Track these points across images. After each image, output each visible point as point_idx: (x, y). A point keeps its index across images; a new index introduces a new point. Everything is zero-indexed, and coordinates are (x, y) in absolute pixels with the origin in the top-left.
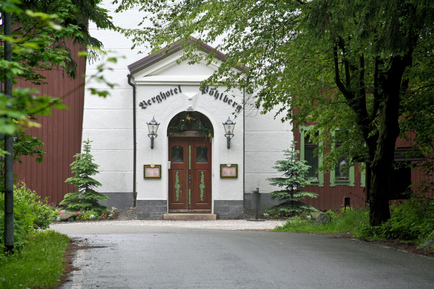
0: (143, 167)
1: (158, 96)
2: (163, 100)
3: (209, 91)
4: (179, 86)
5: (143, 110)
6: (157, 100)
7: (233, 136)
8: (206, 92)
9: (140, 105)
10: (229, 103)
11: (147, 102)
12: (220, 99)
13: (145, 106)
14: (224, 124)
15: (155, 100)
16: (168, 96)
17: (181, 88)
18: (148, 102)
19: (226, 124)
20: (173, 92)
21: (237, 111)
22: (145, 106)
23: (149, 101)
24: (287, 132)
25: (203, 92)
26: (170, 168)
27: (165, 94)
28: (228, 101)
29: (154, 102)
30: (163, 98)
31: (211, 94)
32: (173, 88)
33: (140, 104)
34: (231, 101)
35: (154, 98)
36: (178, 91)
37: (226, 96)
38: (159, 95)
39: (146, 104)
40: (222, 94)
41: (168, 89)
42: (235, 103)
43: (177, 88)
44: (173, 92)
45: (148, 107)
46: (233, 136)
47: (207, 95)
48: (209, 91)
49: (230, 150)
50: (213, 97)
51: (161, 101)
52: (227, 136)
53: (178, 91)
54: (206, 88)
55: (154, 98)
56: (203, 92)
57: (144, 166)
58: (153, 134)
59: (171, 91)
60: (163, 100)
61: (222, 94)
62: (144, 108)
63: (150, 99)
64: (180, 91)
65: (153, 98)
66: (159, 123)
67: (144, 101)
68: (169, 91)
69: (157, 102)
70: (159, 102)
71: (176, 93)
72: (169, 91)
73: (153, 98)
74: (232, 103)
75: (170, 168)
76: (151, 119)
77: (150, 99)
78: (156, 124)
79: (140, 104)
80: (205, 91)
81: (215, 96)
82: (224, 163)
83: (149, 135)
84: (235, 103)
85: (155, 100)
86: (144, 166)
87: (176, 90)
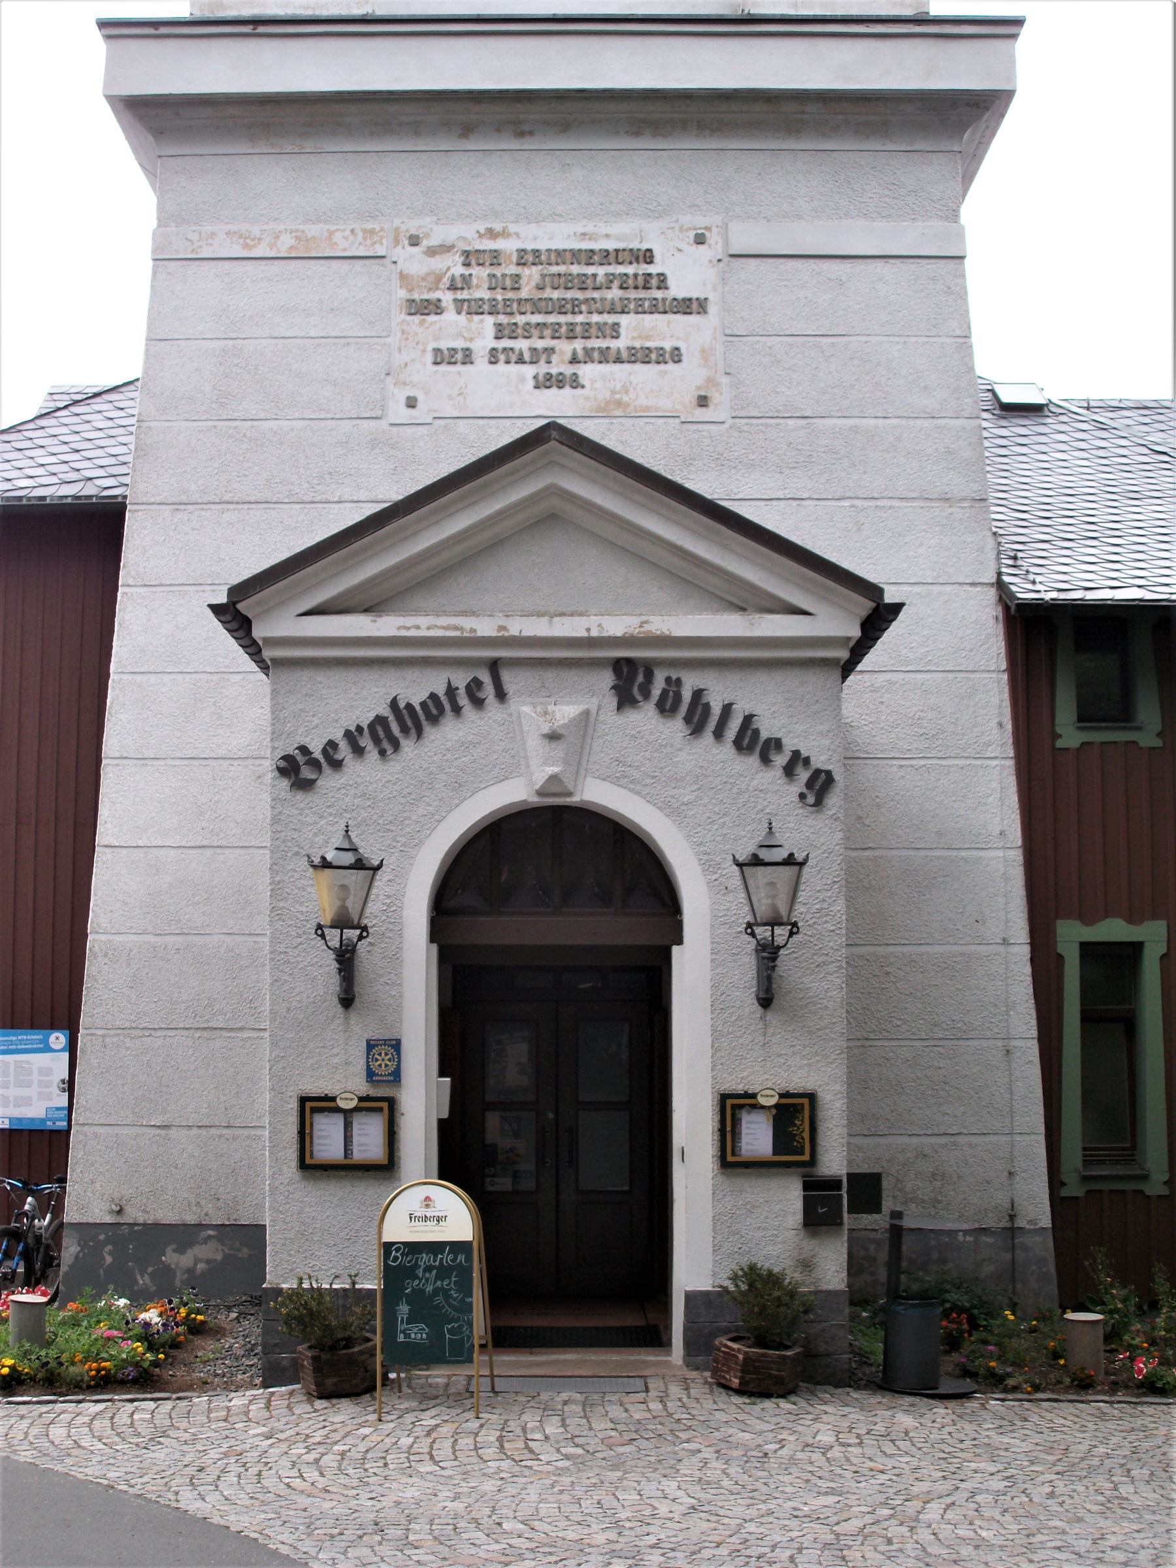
0: (294, 1105)
1: (380, 720)
2: (407, 745)
3: (656, 692)
4: (494, 666)
5: (300, 796)
6: (376, 741)
7: (791, 934)
8: (639, 698)
9: (282, 772)
10: (765, 760)
11: (317, 754)
12: (718, 734)
13: (307, 773)
14: (740, 865)
15: (366, 741)
16: (434, 720)
17: (506, 676)
18: (324, 751)
19: (756, 861)
20: (463, 700)
21: (811, 799)
22: (307, 773)
23: (332, 744)
24: (1001, 949)
25: (625, 699)
26: (445, 1115)
27: (418, 708)
28: (758, 749)
29: (358, 751)
30: (405, 730)
31: (667, 706)
32: (461, 680)
33: (283, 764)
34: (777, 744)
35: (359, 729)
36: (489, 691)
37: (748, 719)
38: (385, 711)
39: (315, 764)
40: (727, 709)
41: (435, 682)
42: (796, 754)
43: (485, 677)
44: (463, 700)
45: (328, 781)
46: (791, 934)
47: (645, 717)
48: (656, 692)
49: (770, 1015)
50: (676, 727)
51: (396, 745)
52: (763, 932)
53: (489, 691)
54: (640, 678)
55: (359, 729)
56: (625, 699)
57: (303, 1100)
58: (342, 922)
59: (451, 691)
60: (407, 745)
61: (727, 709)
62: (305, 786)
63: (338, 735)
64: (501, 695)
65: (353, 729)
66: (376, 863)
67: (304, 750)
68: (441, 691)
69: (372, 754)
70: (382, 753)
71: (478, 703)
72: (441, 691)
73: (353, 729)
74: (781, 760)
75: (445, 1115)
76: (338, 840)
77: (338, 735)
78: (360, 865)
79: (283, 764)
80: (636, 691)
81: (688, 720)
82: (740, 1088)
83: (320, 927)
84: (797, 760)
85: (366, 741)
86: (303, 1100)
87: (474, 688)
